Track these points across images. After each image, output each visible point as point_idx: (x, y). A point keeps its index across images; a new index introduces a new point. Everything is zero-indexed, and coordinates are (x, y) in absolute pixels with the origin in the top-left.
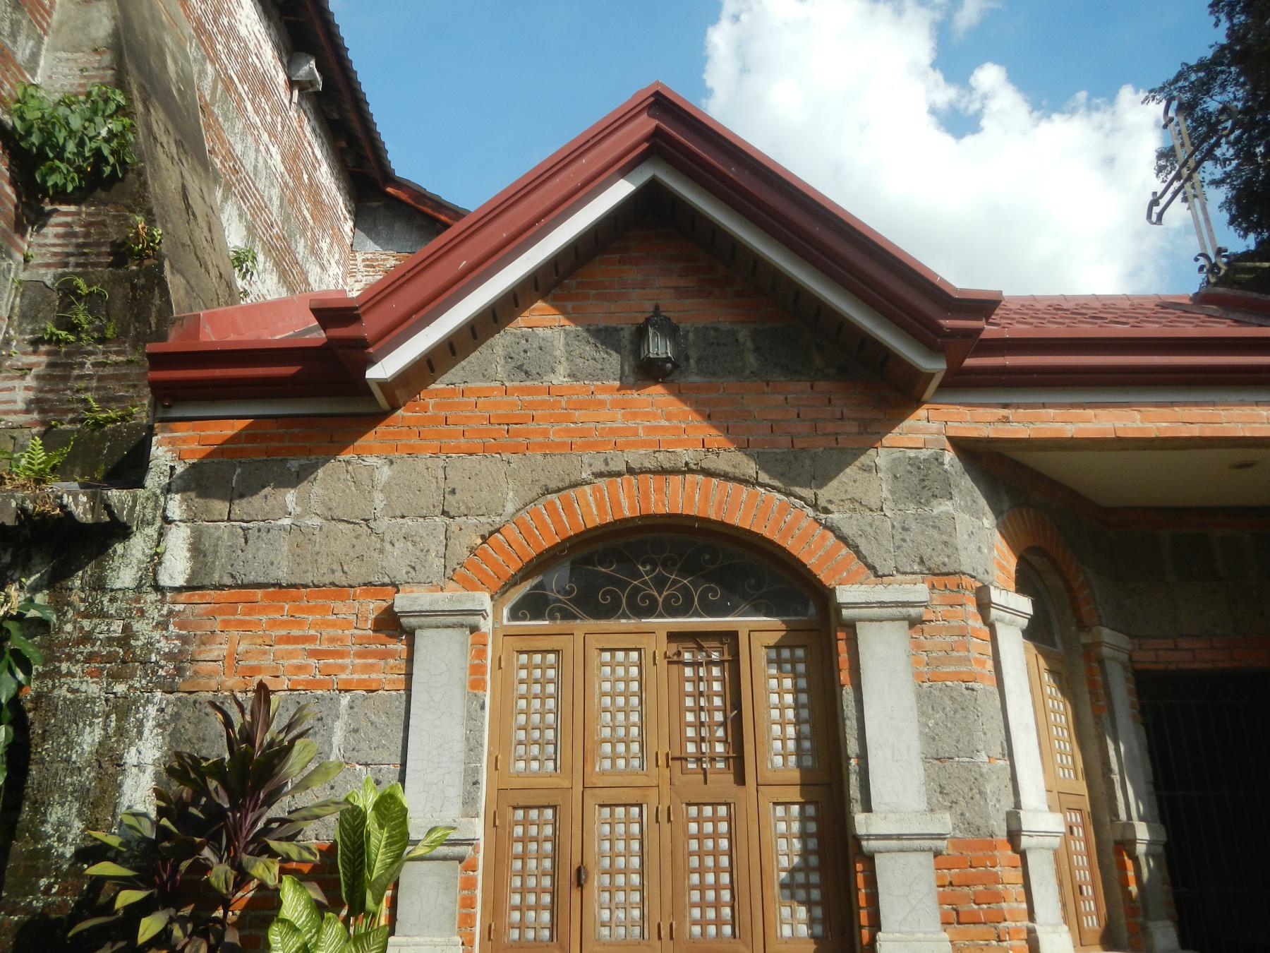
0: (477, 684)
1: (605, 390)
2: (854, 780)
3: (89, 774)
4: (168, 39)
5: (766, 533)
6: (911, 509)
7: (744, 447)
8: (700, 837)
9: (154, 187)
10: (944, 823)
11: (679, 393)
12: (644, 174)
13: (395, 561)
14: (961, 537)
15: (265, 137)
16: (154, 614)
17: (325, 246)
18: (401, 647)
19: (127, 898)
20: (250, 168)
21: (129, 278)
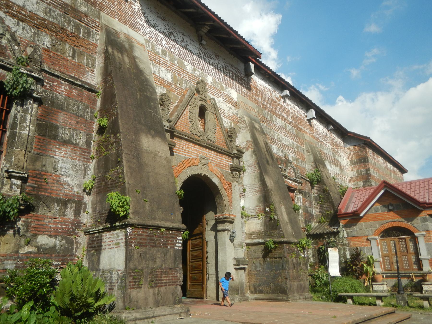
0: (378, 245)
1: (385, 213)
2: (419, 253)
3: (343, 255)
4: (316, 149)
5: (406, 227)
6: (423, 223)
7: (402, 218)
8: (404, 259)
9: (325, 181)
10: (429, 257)
11: (394, 212)
12: (385, 189)
13: (367, 233)
14: (429, 226)
15: (327, 144)
16: (345, 240)
17: (340, 152)
18: (369, 242)
19: (351, 265)
20: (327, 153)
21: (326, 194)
